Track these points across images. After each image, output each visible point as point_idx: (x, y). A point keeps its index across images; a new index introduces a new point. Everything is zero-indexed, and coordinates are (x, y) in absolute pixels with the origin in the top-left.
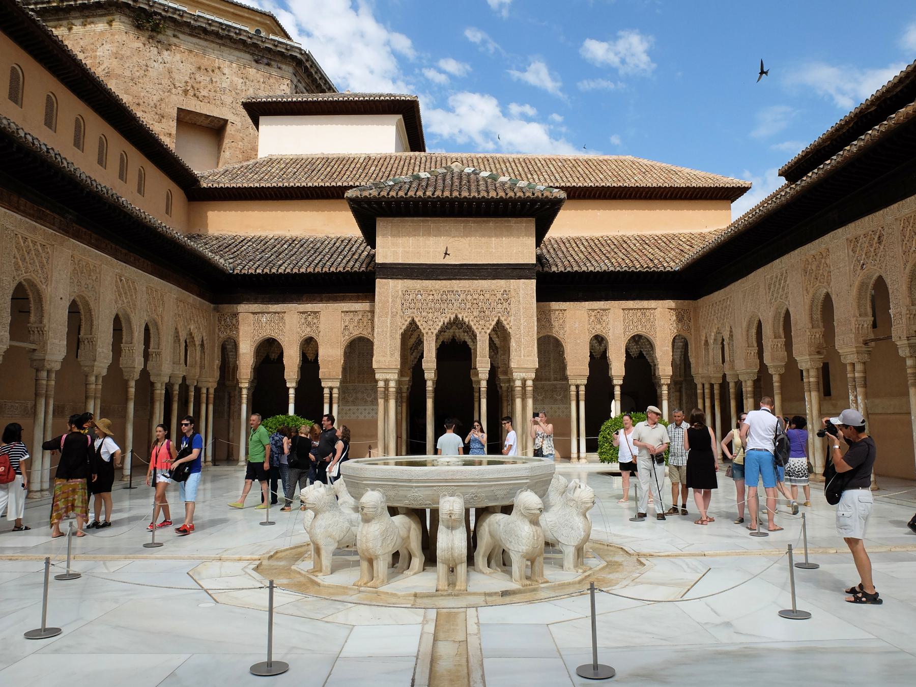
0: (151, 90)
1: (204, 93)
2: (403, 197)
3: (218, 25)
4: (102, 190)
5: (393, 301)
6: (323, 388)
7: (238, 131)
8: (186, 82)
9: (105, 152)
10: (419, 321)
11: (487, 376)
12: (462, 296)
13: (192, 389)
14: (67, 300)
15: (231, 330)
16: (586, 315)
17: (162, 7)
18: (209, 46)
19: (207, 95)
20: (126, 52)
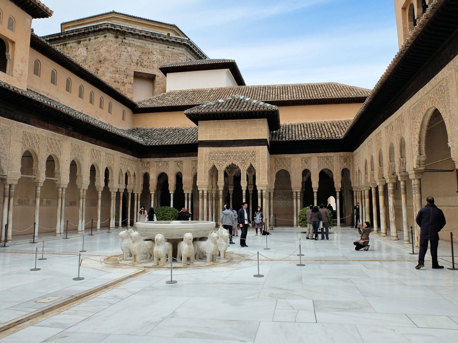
0: (122, 65)
1: (145, 63)
3: (150, 33)
4: (81, 118)
6: (184, 194)
7: (161, 79)
8: (138, 60)
10: (216, 165)
11: (222, 188)
12: (235, 154)
13: (130, 194)
14: (69, 161)
16: (300, 160)
17: (126, 28)
18: (147, 43)
19: (146, 64)
20: (112, 49)
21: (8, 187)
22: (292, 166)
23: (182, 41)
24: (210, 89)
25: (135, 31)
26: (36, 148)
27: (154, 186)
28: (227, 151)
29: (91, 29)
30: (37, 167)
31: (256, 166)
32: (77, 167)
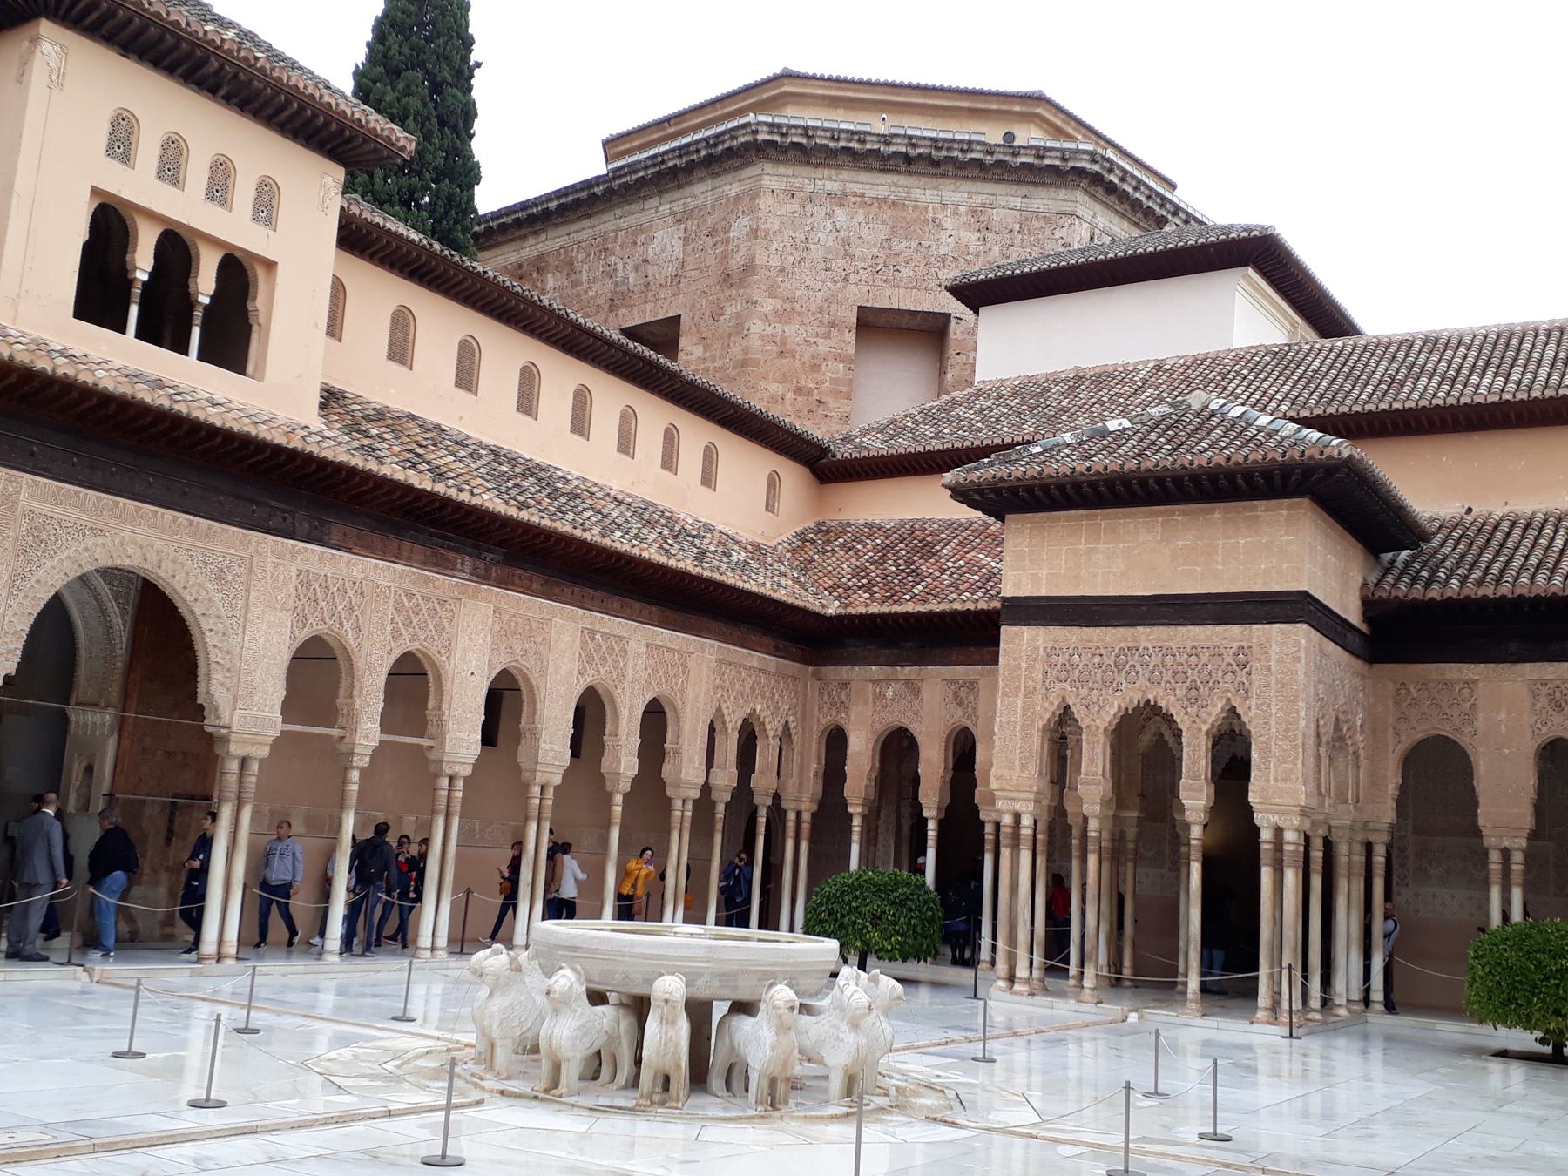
2: (1036, 478)
3: (929, 143)
5: (1029, 666)
6: (983, 823)
9: (633, 432)
12: (1156, 660)
14: (486, 673)
15: (839, 712)
17: (828, 134)
19: (912, 274)
21: (234, 766)
22: (1480, 723)
23: (1064, 159)
24: (1151, 365)
25: (864, 142)
26: (347, 626)
27: (864, 784)
28: (1122, 645)
29: (698, 151)
30: (351, 696)
31: (1250, 714)
32: (525, 698)
